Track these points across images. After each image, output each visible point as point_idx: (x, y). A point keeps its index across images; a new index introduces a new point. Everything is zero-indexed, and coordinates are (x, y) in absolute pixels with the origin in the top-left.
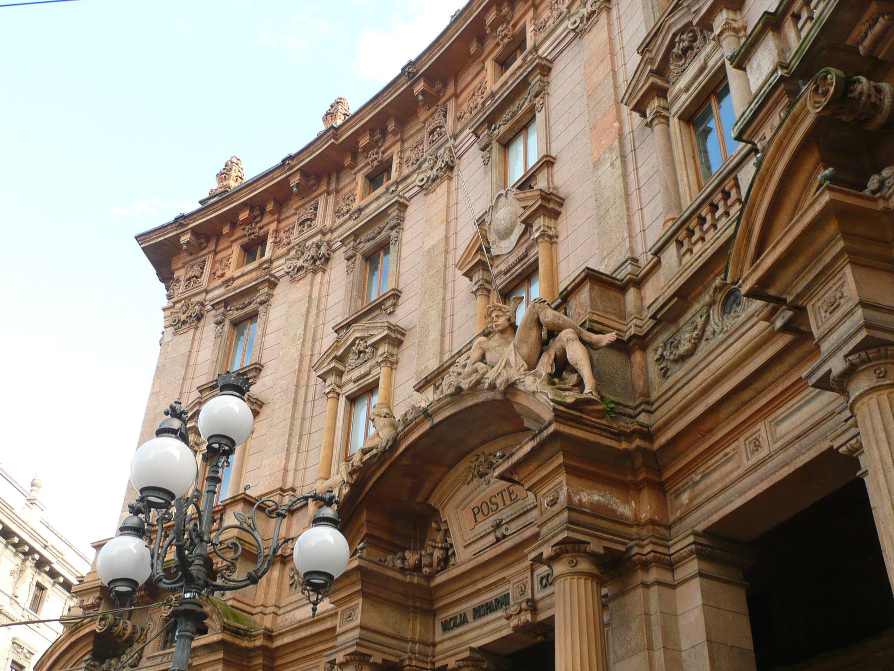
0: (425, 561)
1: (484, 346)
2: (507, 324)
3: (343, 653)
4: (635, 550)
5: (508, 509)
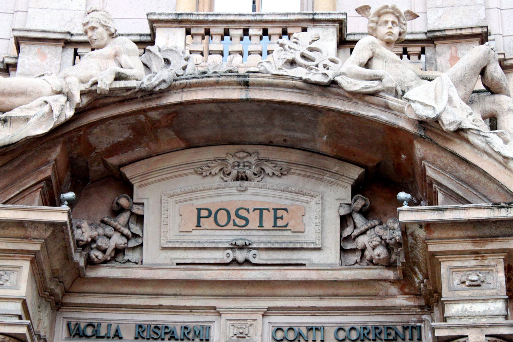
1: (378, 51)
5: (262, 233)
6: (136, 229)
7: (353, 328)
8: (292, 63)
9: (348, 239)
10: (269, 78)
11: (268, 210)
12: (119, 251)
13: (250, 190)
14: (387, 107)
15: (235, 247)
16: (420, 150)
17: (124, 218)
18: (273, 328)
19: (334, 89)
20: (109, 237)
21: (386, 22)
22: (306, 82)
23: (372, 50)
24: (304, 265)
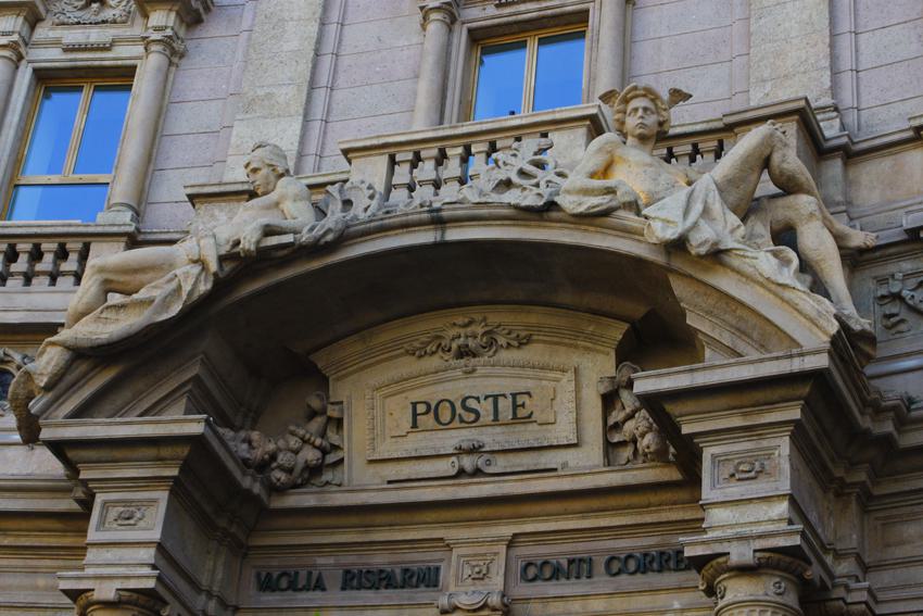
0: (282, 458)
2: (656, 129)
3: (118, 584)
4: (840, 592)
5: (498, 429)
6: (333, 437)
7: (630, 556)
8: (507, 184)
9: (617, 426)
10: (470, 208)
11: (504, 396)
12: (314, 471)
13: (480, 371)
14: (627, 232)
15: (461, 451)
16: (679, 288)
17: (319, 421)
18: (524, 563)
19: (554, 215)
20: (296, 452)
21: (636, 110)
22: (516, 207)
23: (610, 152)
24: (555, 470)
